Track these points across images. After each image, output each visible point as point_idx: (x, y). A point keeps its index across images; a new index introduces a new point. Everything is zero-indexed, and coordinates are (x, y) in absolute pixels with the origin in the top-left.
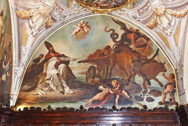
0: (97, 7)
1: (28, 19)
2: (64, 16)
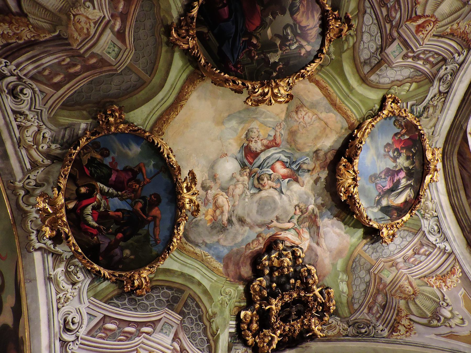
0: (75, 196)
2: (22, 91)
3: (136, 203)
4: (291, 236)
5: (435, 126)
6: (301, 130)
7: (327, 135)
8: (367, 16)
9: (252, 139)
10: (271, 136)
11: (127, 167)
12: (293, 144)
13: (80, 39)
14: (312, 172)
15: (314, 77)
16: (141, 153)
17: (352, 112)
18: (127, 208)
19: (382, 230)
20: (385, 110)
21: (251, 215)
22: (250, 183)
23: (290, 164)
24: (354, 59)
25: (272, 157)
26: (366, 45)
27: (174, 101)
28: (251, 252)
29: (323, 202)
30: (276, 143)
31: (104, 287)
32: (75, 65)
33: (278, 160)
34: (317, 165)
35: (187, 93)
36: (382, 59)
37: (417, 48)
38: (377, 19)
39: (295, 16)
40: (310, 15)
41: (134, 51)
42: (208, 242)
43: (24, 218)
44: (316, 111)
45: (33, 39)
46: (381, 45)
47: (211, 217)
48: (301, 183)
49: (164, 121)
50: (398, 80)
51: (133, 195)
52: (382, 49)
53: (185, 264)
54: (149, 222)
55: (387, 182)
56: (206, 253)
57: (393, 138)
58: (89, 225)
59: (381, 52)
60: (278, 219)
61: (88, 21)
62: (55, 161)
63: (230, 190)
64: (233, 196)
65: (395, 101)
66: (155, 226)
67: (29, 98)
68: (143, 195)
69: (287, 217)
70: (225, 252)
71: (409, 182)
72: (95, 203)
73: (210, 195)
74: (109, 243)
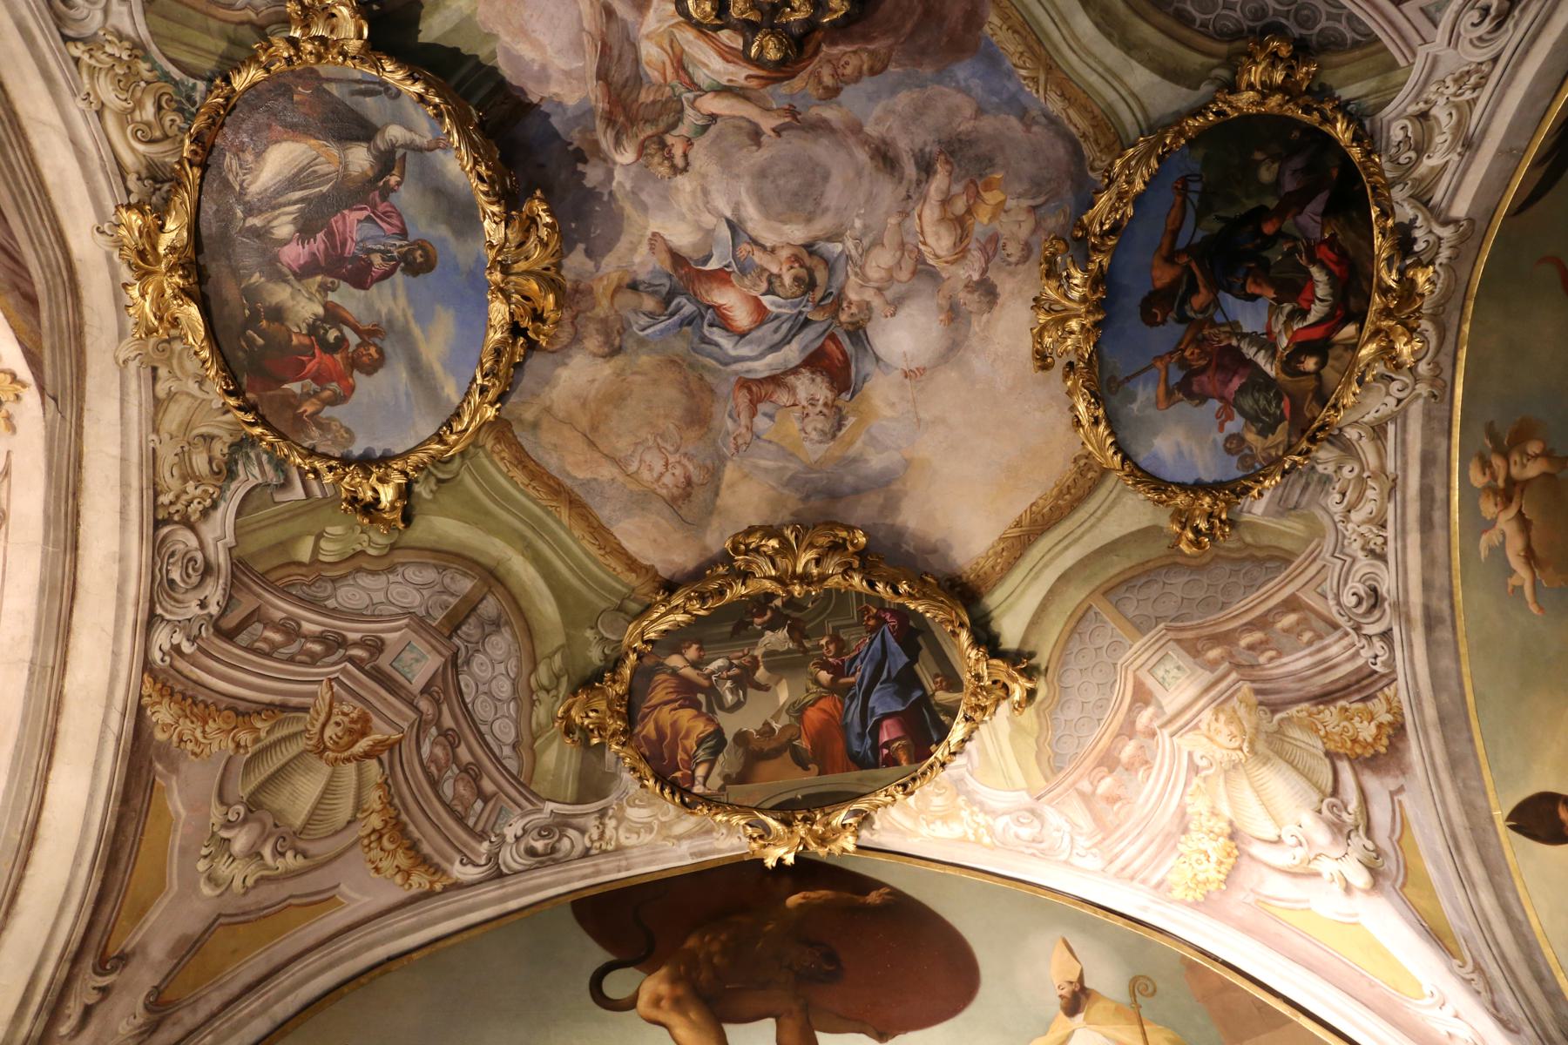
0: (1333, 353)
1: (1244, 861)
2: (1359, 603)
3: (1203, 310)
4: (711, 64)
5: (158, 403)
6: (671, 426)
7: (584, 405)
8: (510, 737)
9: (825, 411)
10: (765, 415)
11: (1197, 405)
12: (694, 386)
13: (1235, 702)
14: (620, 279)
15: (641, 580)
16: (1155, 434)
17: (511, 479)
18: (1229, 301)
19: (363, 46)
20: (399, 484)
21: (851, 174)
22: (840, 277)
23: (703, 317)
24: (529, 632)
25: (763, 347)
26: (501, 668)
27: (1036, 539)
28: (867, 38)
29: (580, 167)
30: (750, 390)
31: (1358, 85)
32: (1251, 647)
33: (742, 335)
34: (605, 302)
35: (998, 554)
36: (450, 637)
37: (344, 671)
38: (482, 735)
39: (710, 729)
40: (669, 731)
41: (1120, 662)
42: (1014, 121)
43: (1442, 305)
44: (633, 487)
45: (1321, 707)
46: (457, 675)
47: (987, 196)
48: (659, 246)
49: (1069, 492)
50: (373, 573)
51: (1206, 332)
52: (454, 664)
53: (1110, 75)
54: (1189, 249)
55: (356, 236)
56: (1029, 88)
57: (352, 389)
58: (1330, 273)
59: (455, 656)
60: (756, 135)
61: (1212, 733)
62: (1336, 432)
63: (911, 268)
64: (902, 245)
65: (370, 509)
66: (1175, 234)
67: (1350, 584)
68: (1183, 327)
69: (720, 136)
70: (963, 71)
71: (256, 221)
72: (1295, 328)
73: (977, 266)
74: (1300, 213)
